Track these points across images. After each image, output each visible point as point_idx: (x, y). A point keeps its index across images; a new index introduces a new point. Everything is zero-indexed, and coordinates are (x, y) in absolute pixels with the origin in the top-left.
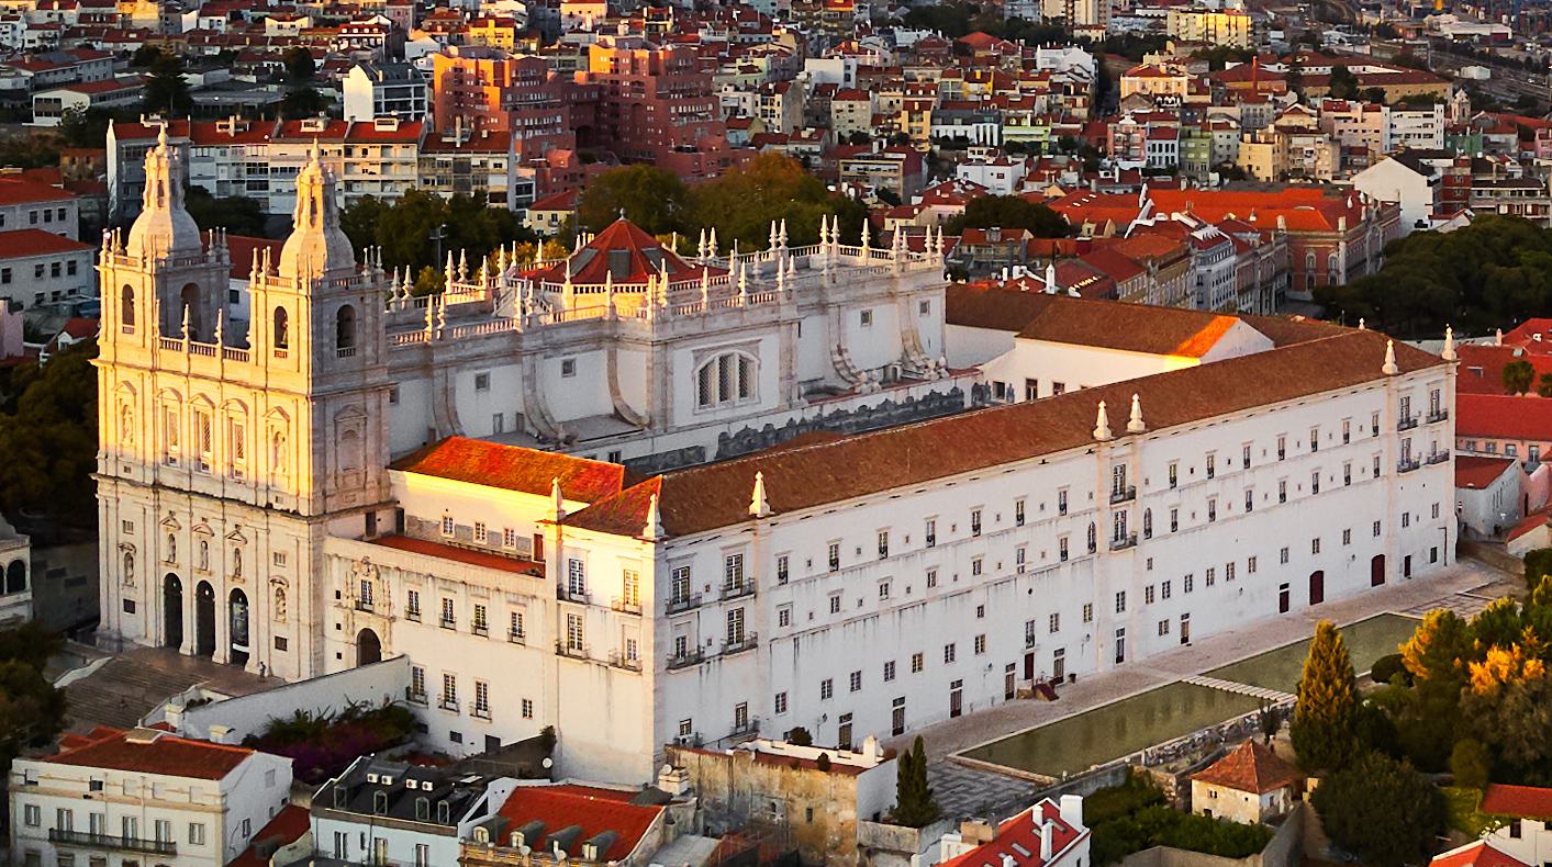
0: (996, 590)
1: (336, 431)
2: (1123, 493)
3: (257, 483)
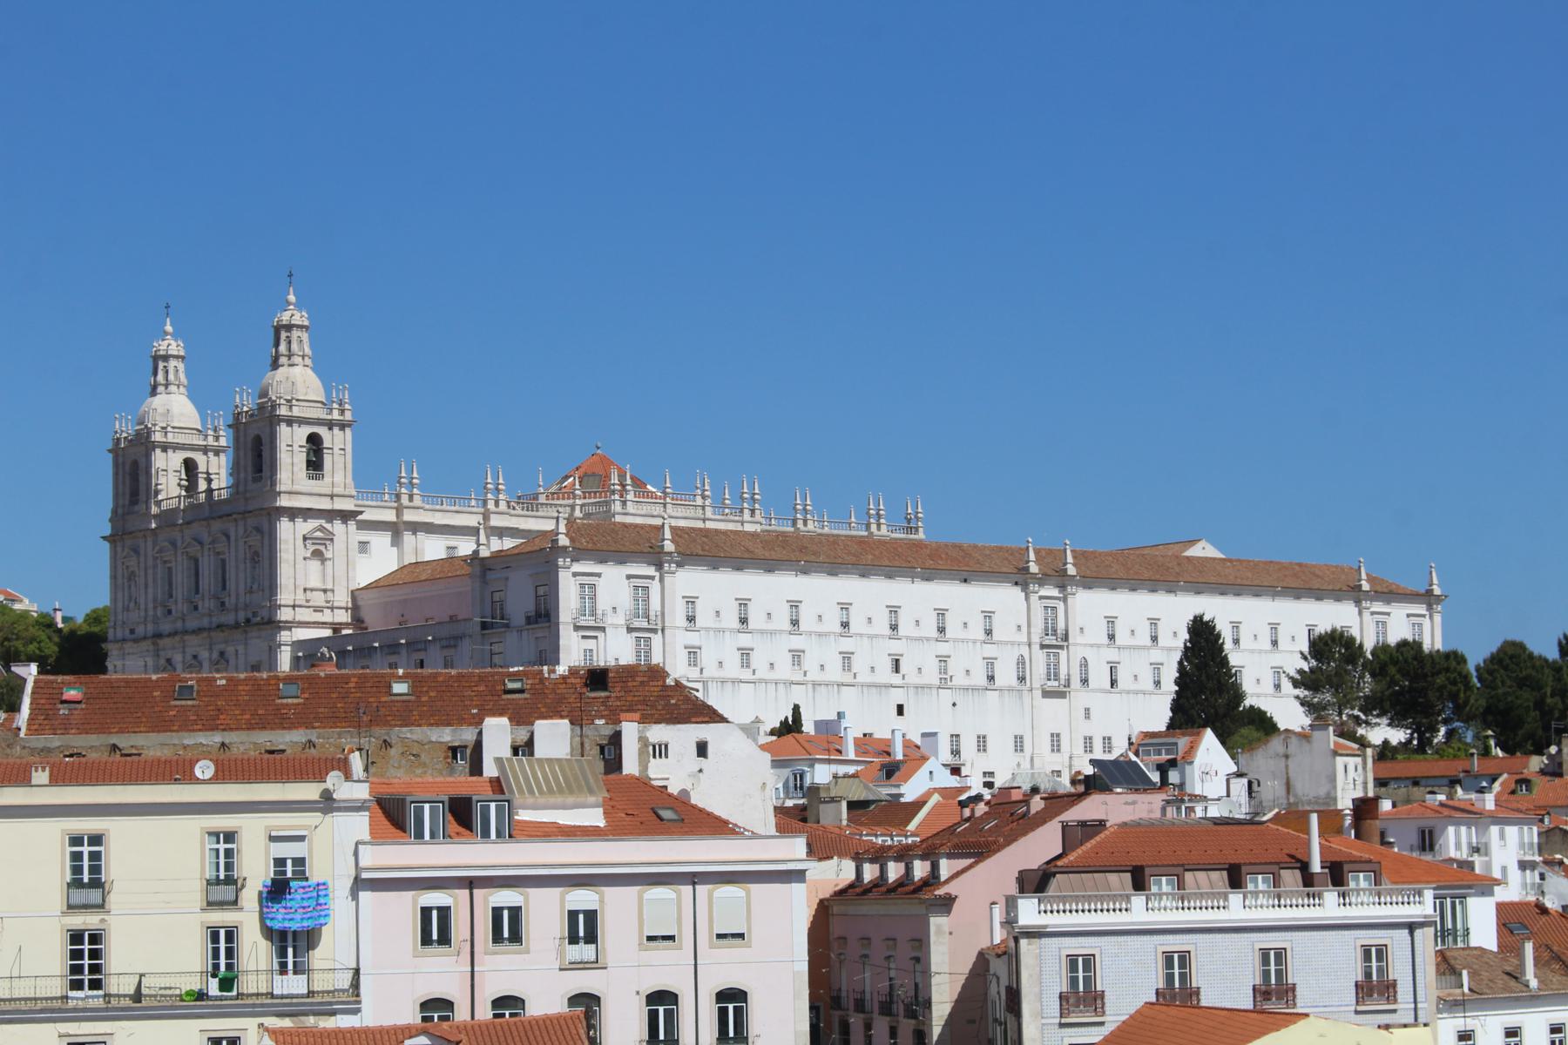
0: (917, 693)
1: (305, 546)
2: (1057, 640)
3: (236, 605)
